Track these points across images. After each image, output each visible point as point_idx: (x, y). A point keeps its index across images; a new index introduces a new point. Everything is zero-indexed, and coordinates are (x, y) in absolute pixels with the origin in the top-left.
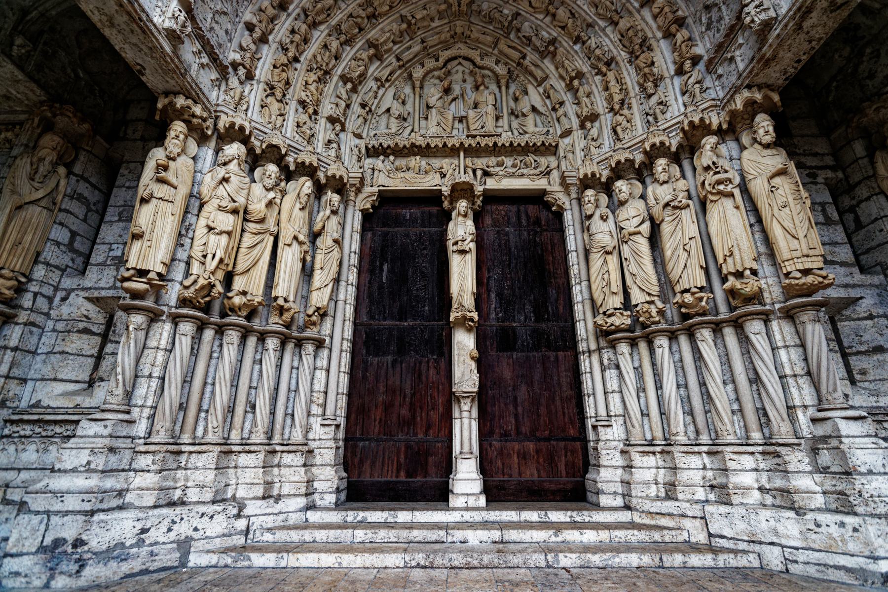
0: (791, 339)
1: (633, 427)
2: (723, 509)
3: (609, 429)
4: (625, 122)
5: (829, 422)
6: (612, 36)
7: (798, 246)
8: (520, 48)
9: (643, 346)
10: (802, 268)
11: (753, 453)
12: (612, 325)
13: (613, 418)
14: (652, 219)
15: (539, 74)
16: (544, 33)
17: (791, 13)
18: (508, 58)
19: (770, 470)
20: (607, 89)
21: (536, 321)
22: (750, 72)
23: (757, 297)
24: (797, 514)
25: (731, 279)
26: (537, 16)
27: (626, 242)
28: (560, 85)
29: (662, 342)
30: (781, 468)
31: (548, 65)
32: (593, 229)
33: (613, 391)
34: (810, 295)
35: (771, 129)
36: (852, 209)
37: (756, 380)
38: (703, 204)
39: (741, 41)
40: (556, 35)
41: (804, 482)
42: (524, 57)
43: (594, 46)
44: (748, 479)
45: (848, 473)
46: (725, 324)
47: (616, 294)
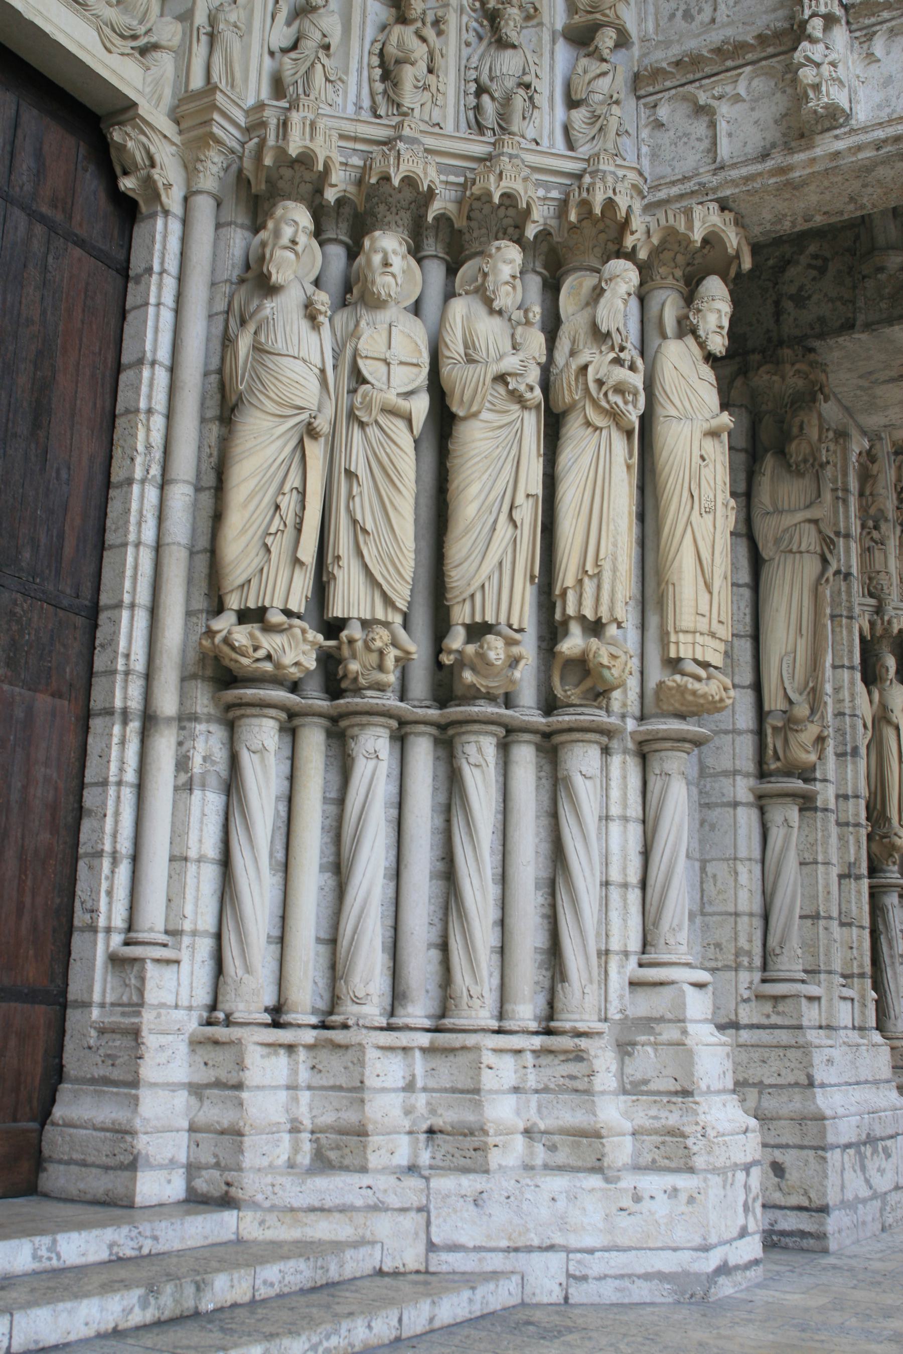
1: (248, 970)
2: (469, 1183)
3: (169, 972)
5: (666, 991)
7: (708, 607)
9: (314, 740)
10: (700, 658)
11: (519, 1052)
12: (269, 657)
13: (186, 940)
17: (880, 134)
19: (546, 1090)
22: (747, 179)
24: (607, 1180)
27: (362, 425)
30: (578, 1084)
35: (726, 323)
39: (741, 89)
41: (612, 1112)
45: (686, 1093)
46: (527, 737)
47: (302, 564)
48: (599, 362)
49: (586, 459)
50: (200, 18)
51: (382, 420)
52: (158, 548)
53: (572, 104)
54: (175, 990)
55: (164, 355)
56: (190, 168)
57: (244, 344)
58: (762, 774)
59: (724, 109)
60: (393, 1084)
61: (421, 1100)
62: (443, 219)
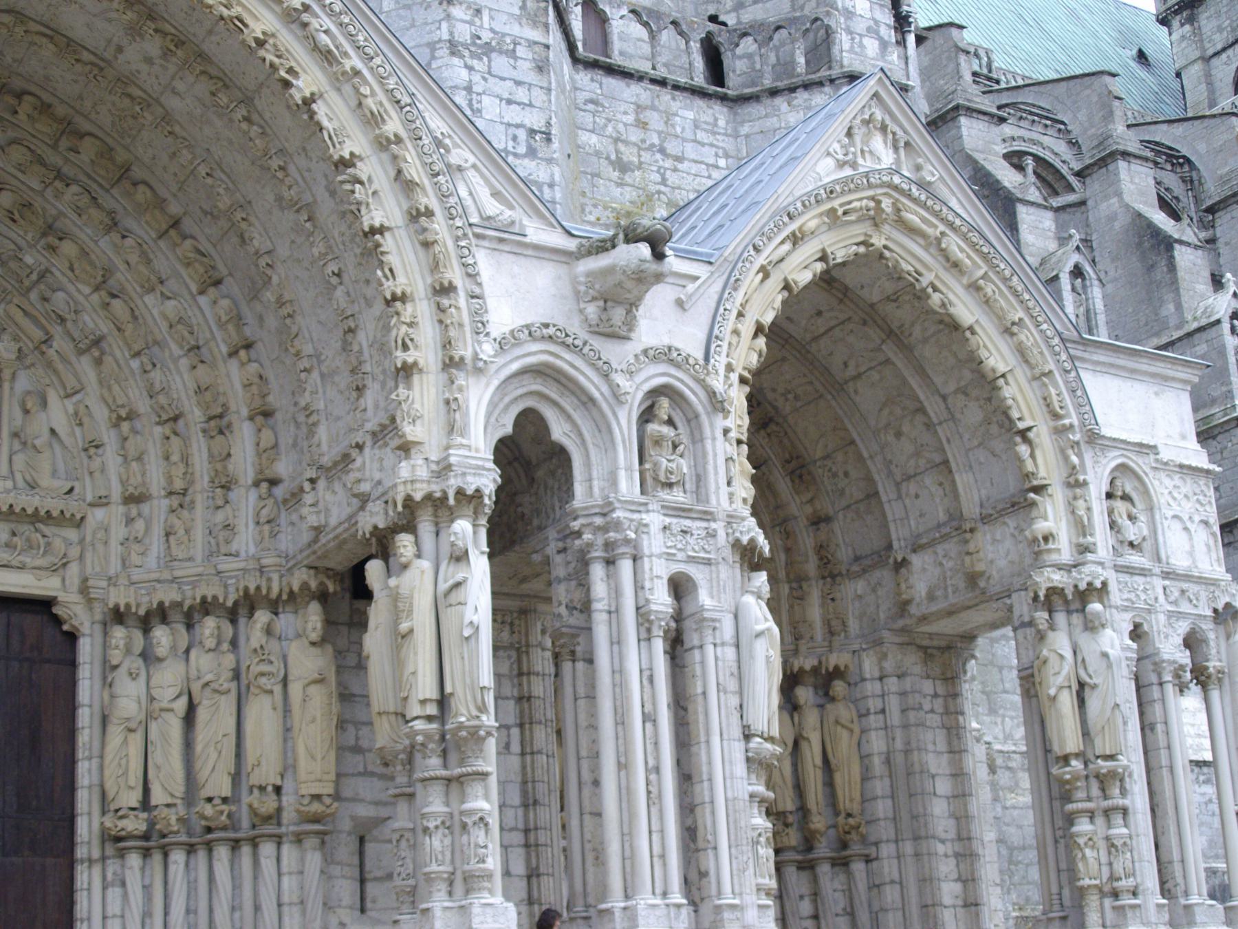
4: (182, 532)
6: (186, 376)
8: (43, 321)
9: (157, 857)
15: (71, 383)
18: (20, 329)
20: (167, 458)
23: (275, 817)
26: (80, 286)
28: (101, 413)
29: (178, 857)
31: (85, 365)
32: (118, 689)
33: (114, 916)
35: (319, 625)
40: (105, 331)
42: (47, 341)
43: (158, 387)
51: (163, 714)
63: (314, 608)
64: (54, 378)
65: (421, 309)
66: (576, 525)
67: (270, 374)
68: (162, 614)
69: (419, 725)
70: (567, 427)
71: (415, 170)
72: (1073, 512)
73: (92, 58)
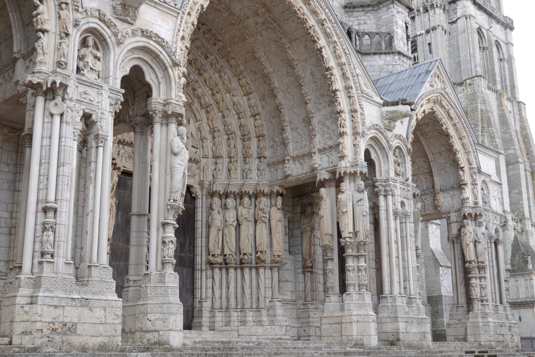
0: (270, 276)
2: (244, 327)
3: (206, 303)
9: (224, 271)
14: (238, 220)
15: (198, 117)
16: (206, 98)
21: (181, 252)
23: (264, 261)
25: (259, 252)
28: (207, 128)
29: (232, 271)
34: (277, 263)
36: (292, 230)
37: (258, 287)
38: (256, 221)
40: (212, 103)
44: (250, 319)
48: (260, 213)
49: (259, 228)
50: (202, 168)
52: (201, 247)
53: (258, 170)
54: (207, 305)
55: (200, 219)
56: (202, 191)
57: (210, 218)
58: (304, 268)
59: (279, 170)
60: (235, 315)
61: (239, 318)
62: (238, 193)
63: (279, 198)
64: (193, 115)
65: (346, 116)
66: (377, 184)
67: (264, 124)
68: (226, 195)
69: (348, 239)
70: (376, 155)
71: (349, 74)
72: (473, 192)
73: (237, 19)
